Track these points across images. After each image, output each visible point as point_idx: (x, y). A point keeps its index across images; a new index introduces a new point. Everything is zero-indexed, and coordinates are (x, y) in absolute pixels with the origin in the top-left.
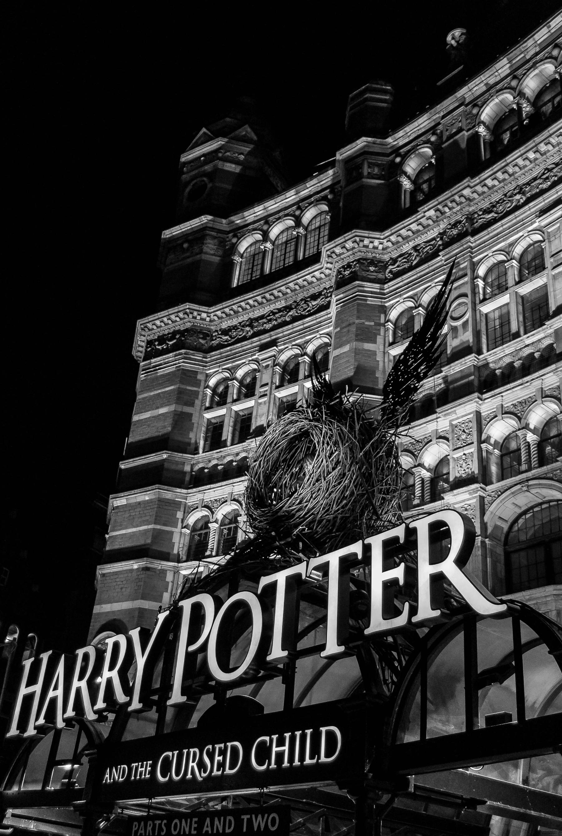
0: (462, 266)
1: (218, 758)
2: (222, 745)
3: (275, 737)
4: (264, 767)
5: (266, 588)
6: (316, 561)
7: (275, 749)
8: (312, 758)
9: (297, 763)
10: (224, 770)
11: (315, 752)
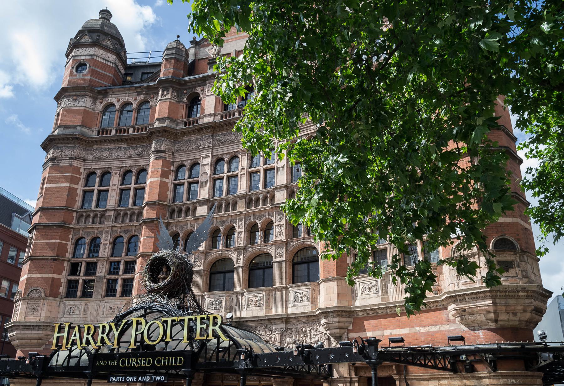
11: (176, 362)
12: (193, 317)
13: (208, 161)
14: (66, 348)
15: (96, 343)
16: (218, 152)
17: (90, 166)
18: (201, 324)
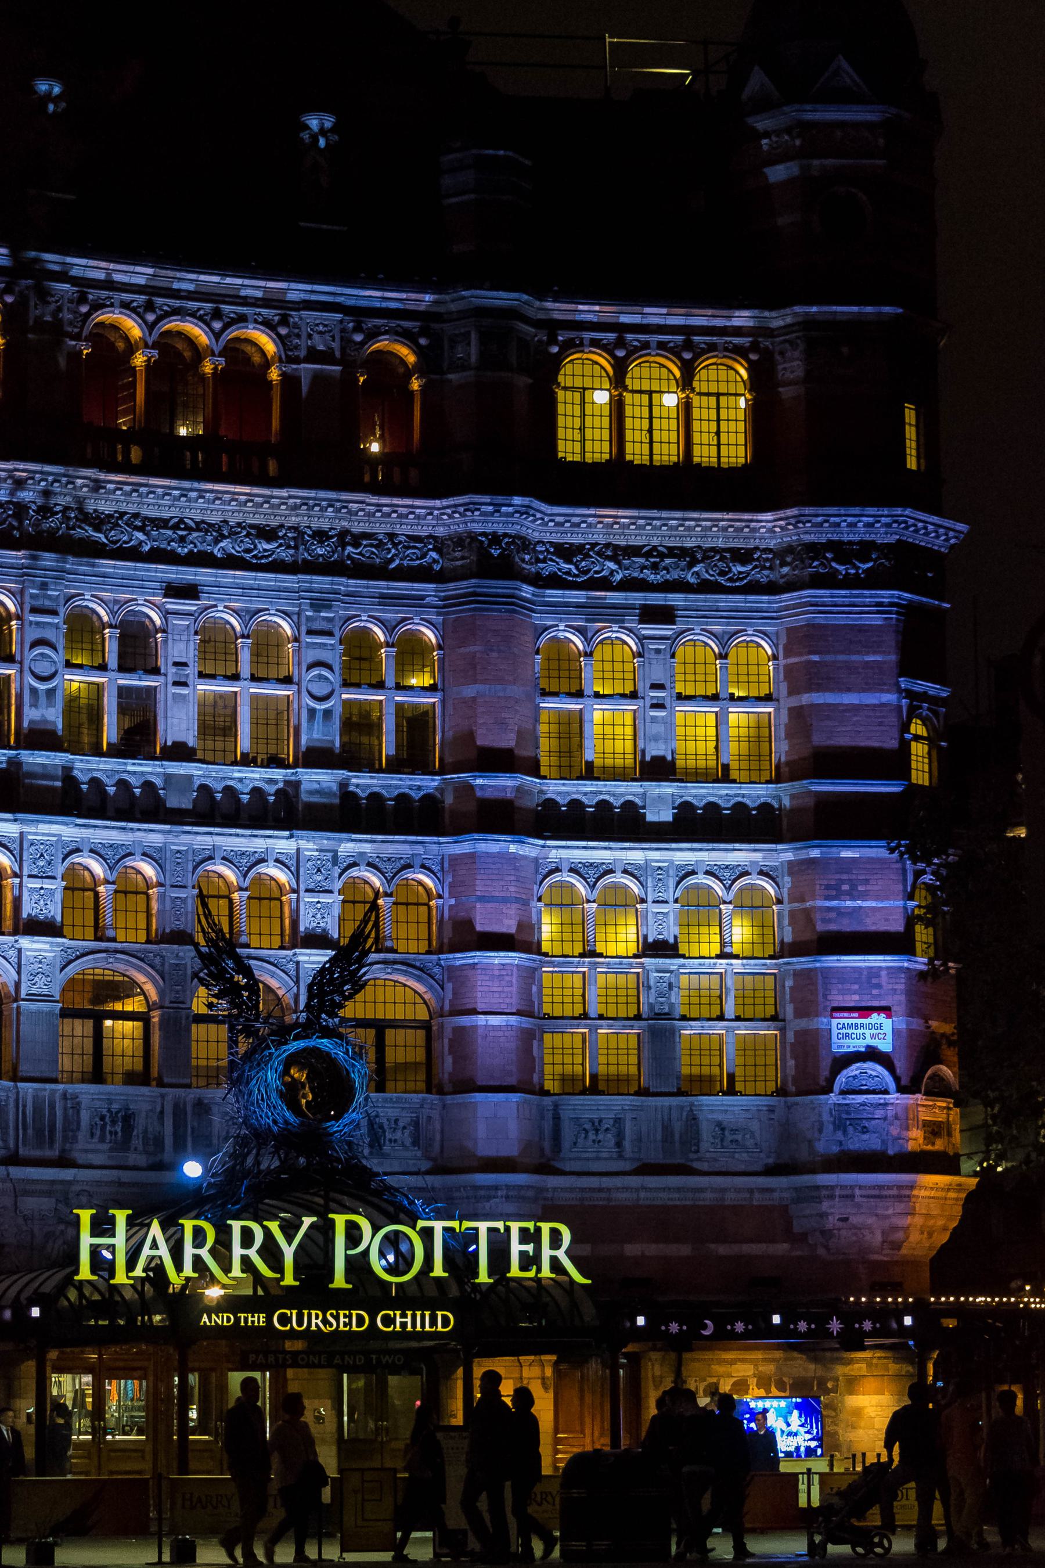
0: (49, 593)
1: (342, 1320)
2: (347, 1312)
3: (398, 1313)
4: (391, 1329)
5: (423, 1229)
6: (467, 1224)
7: (398, 1320)
8: (431, 1326)
9: (418, 1328)
10: (351, 1327)
11: (433, 1322)
12: (500, 1225)
14: (128, 1277)
15: (179, 1267)
18: (522, 1241)
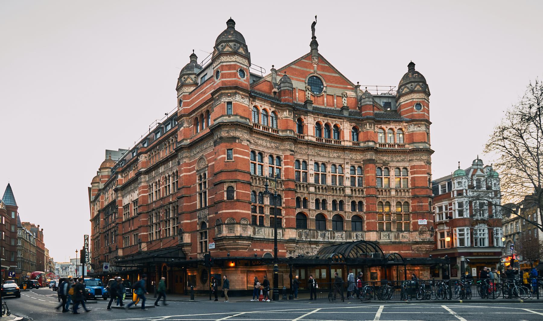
13: (313, 163)
16: (318, 159)
17: (253, 147)
